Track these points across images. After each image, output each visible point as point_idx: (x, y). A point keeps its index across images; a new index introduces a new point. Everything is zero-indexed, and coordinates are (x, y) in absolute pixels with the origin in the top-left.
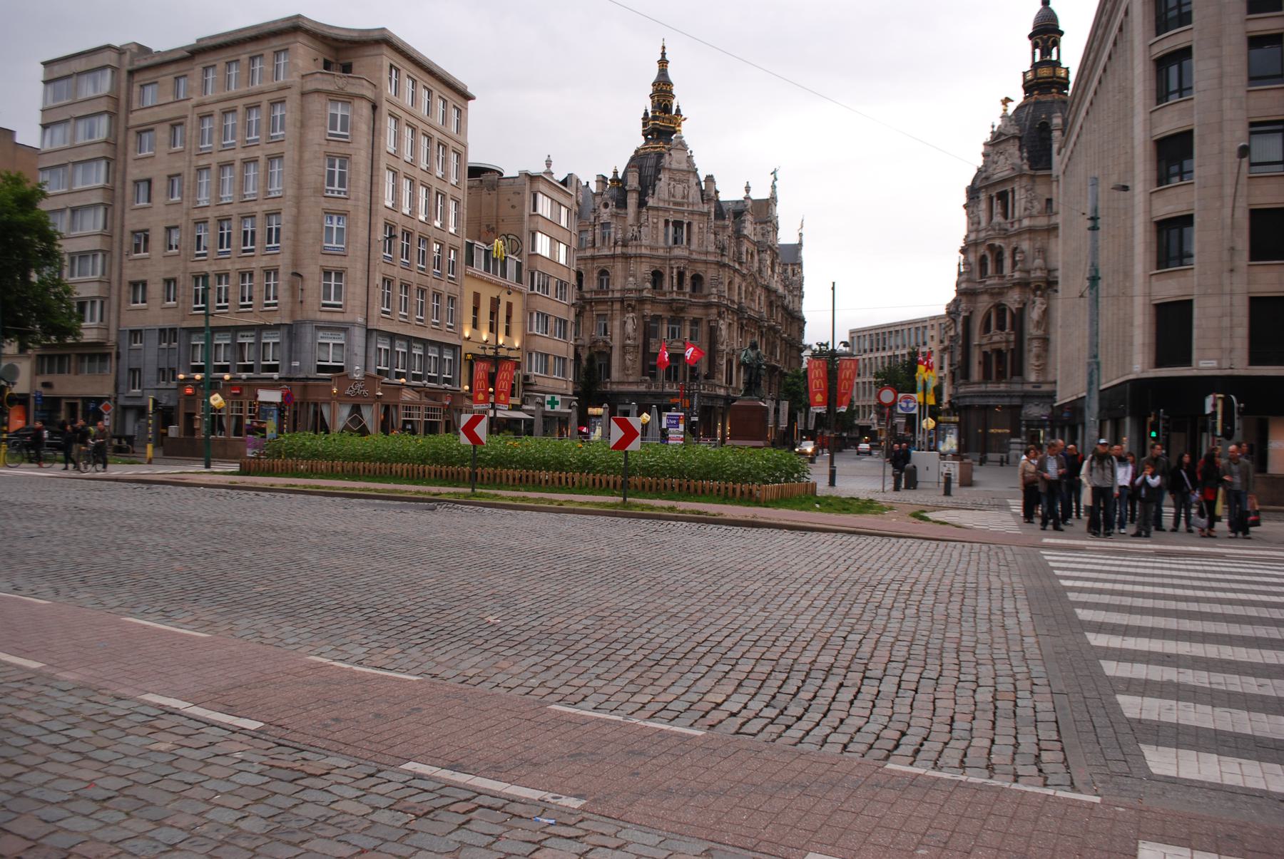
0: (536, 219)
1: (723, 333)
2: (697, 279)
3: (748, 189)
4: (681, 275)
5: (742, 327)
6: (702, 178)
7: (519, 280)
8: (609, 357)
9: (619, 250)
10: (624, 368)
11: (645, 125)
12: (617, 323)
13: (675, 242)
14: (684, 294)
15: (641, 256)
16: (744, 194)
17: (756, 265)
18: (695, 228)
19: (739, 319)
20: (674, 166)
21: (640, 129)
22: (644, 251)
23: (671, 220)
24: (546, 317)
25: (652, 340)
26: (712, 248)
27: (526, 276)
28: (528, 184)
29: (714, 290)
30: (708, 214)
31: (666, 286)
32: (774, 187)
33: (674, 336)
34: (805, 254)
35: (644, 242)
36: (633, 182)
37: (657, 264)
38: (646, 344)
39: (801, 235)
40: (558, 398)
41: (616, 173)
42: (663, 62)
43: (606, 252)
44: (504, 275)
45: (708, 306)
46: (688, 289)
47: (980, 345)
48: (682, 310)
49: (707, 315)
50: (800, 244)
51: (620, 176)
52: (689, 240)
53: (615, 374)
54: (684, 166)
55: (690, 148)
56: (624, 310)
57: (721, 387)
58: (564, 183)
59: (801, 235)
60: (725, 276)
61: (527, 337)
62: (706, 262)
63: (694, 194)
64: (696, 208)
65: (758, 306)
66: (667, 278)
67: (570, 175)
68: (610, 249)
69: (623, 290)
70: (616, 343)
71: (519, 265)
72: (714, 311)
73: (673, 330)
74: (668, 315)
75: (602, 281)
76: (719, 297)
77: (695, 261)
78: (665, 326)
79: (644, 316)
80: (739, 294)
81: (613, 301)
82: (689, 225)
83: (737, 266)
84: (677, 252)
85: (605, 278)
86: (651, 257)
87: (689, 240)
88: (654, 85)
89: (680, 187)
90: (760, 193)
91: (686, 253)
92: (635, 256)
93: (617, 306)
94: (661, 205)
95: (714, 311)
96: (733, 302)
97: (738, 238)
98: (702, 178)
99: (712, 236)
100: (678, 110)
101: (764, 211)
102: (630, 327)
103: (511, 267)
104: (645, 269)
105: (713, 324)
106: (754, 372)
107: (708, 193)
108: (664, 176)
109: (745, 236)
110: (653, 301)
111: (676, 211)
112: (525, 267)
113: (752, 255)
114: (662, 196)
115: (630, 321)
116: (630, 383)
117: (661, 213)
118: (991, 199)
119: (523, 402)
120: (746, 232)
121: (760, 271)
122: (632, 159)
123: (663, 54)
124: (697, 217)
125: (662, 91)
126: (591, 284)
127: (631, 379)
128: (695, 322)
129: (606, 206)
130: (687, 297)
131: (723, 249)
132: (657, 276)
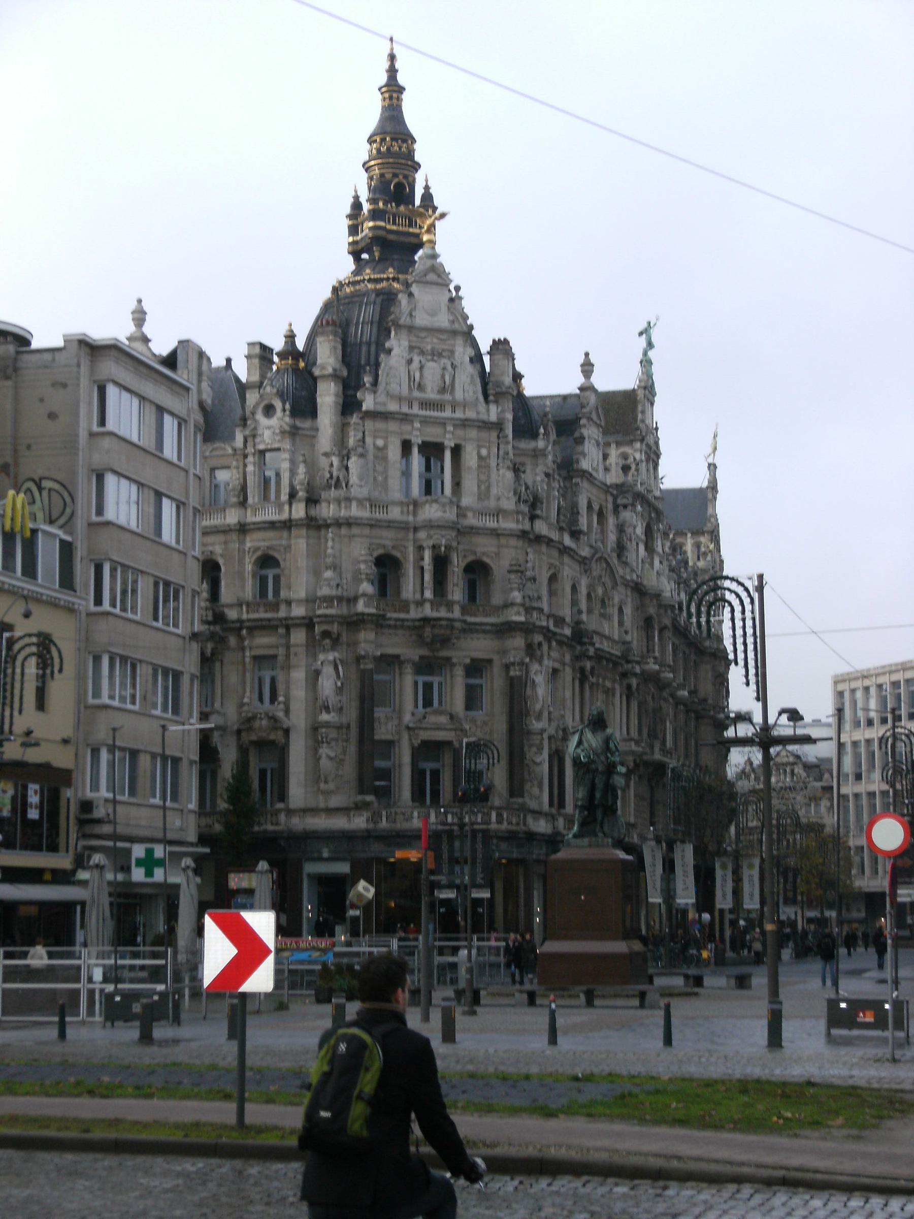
1: (541, 692)
2: (477, 571)
3: (587, 368)
4: (441, 563)
5: (583, 677)
6: (485, 347)
7: (67, 581)
8: (281, 752)
9: (299, 511)
10: (316, 776)
11: (353, 230)
12: (299, 675)
13: (428, 488)
14: (450, 606)
15: (349, 523)
16: (580, 380)
17: (612, 537)
18: (470, 459)
19: (577, 658)
20: (421, 319)
21: (344, 239)
22: (355, 511)
23: (417, 440)
24: (130, 664)
25: (380, 713)
26: (509, 504)
27: (83, 573)
28: (84, 370)
29: (517, 596)
30: (498, 426)
31: (409, 589)
32: (646, 363)
33: (428, 703)
34: (724, 509)
35: (355, 492)
36: (327, 357)
37: (387, 538)
38: (366, 722)
39: (712, 467)
40: (159, 851)
41: (291, 337)
42: (393, 90)
43: (270, 514)
44: (30, 571)
45: (505, 630)
46: (457, 593)
48: (445, 641)
49: (503, 652)
50: (713, 487)
51: (300, 344)
52: (457, 485)
53: (297, 793)
54: (443, 320)
55: (456, 278)
56: (313, 646)
57: (538, 813)
58: (171, 361)
59: (712, 467)
60: (539, 562)
62: (495, 533)
63: (466, 385)
64: (471, 414)
66: (410, 570)
67: (184, 344)
68: (280, 506)
69: (311, 600)
70: (298, 719)
71: (67, 549)
72: (518, 642)
73: (428, 687)
74: (411, 653)
75: (263, 581)
76: (528, 610)
77: (472, 531)
78: (409, 680)
79: (359, 659)
80: (574, 603)
81: (288, 625)
82: (457, 451)
83: (567, 541)
84: (431, 512)
85: (270, 573)
86: (373, 525)
87: (457, 485)
88: (371, 141)
89: (433, 369)
90: (617, 377)
92: (338, 523)
93: (299, 637)
94: (393, 407)
95: (518, 642)
96: (560, 622)
97: (568, 478)
98: (485, 346)
99: (510, 475)
100: (428, 197)
102: (327, 684)
103: (48, 556)
104: (357, 553)
107: (496, 375)
108: (398, 344)
109: (585, 474)
110: (379, 622)
111: (425, 421)
112: (80, 553)
113: (601, 514)
114: (394, 388)
115: (328, 670)
116: (330, 811)
117: (393, 426)
119: (80, 862)
120: (585, 464)
121: (621, 548)
122: (327, 307)
123: (392, 72)
124: (473, 433)
125: (394, 150)
126: (237, 588)
127: (335, 801)
128: (476, 668)
129: (269, 410)
130: (457, 613)
132: (387, 567)
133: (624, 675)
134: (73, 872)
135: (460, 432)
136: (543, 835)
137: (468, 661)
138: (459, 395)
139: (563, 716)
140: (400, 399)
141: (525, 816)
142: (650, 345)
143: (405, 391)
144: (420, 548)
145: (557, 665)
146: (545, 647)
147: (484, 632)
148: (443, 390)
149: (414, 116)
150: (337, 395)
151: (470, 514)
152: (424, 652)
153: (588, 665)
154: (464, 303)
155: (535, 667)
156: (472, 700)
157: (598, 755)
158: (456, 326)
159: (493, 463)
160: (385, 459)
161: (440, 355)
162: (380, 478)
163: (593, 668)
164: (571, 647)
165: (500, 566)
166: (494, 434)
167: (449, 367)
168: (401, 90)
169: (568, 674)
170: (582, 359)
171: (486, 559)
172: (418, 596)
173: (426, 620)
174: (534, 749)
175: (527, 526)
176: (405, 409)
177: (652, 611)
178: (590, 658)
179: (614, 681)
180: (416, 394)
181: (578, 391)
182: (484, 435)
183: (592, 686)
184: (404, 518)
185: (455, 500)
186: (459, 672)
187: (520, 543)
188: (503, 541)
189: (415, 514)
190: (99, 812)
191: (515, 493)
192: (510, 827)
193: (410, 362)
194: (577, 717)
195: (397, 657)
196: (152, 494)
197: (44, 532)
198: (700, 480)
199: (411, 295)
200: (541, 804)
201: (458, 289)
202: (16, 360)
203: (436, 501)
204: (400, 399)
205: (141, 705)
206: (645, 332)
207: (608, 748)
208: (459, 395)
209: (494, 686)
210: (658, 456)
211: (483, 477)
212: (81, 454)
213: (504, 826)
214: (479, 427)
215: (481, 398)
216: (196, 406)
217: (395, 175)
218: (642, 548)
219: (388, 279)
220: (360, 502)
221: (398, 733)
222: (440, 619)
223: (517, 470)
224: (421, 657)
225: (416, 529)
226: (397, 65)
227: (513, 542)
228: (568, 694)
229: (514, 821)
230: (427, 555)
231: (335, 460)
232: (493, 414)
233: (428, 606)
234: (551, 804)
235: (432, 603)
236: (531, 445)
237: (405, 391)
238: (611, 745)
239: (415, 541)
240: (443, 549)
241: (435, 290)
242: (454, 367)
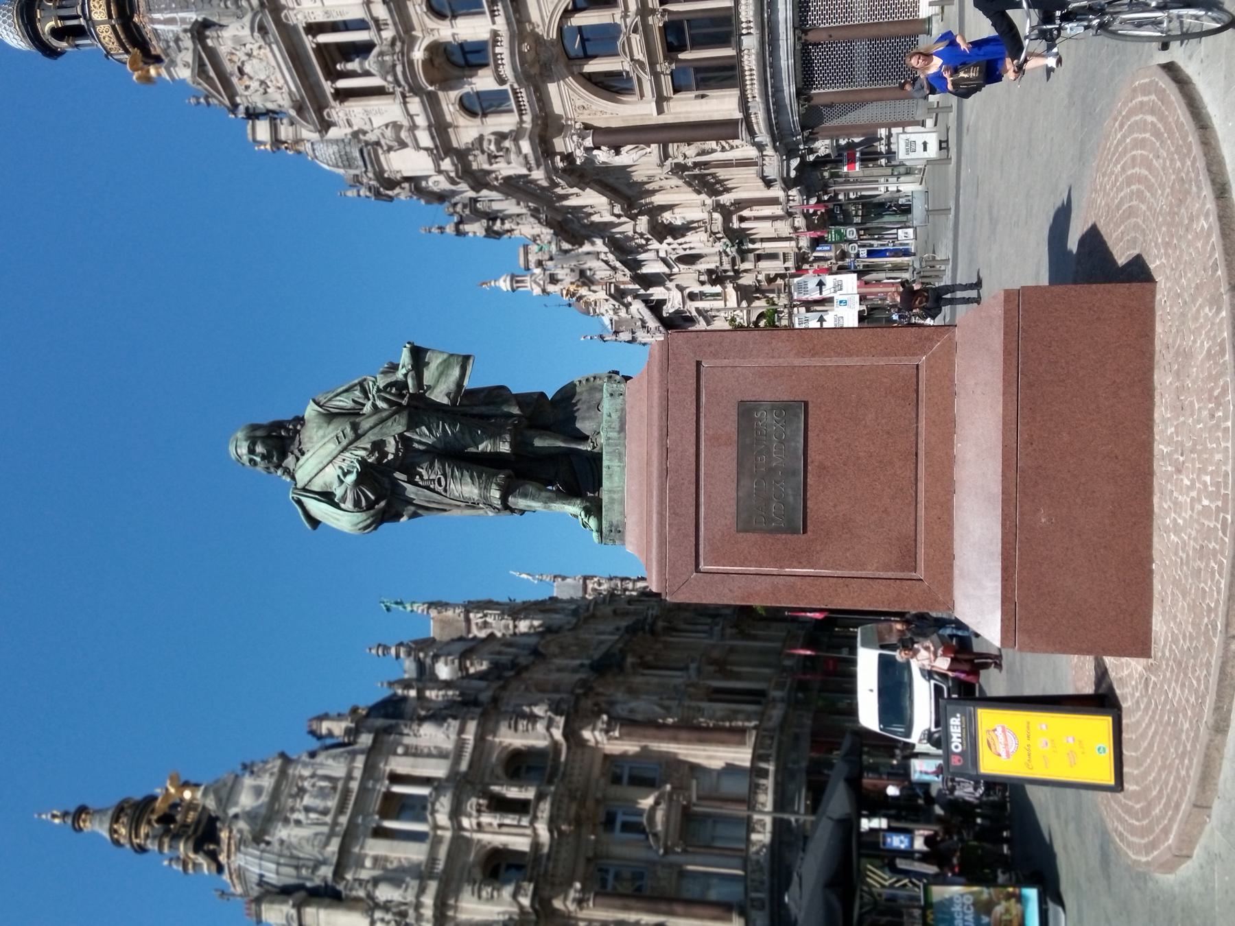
31: (521, 843)
47: (661, 100)
64: (360, 762)
82: (396, 778)
87: (426, 781)
118: (343, 95)
133: (653, 632)
143: (325, 829)
150: (319, 906)
157: (358, 437)
169: (638, 680)
180: (328, 819)
185: (436, 784)
195: (589, 860)
199: (236, 816)
203: (433, 804)
217: (149, 822)
219: (229, 838)
220: (422, 890)
221: (671, 865)
231: (378, 914)
239: (473, 831)
240: (481, 801)
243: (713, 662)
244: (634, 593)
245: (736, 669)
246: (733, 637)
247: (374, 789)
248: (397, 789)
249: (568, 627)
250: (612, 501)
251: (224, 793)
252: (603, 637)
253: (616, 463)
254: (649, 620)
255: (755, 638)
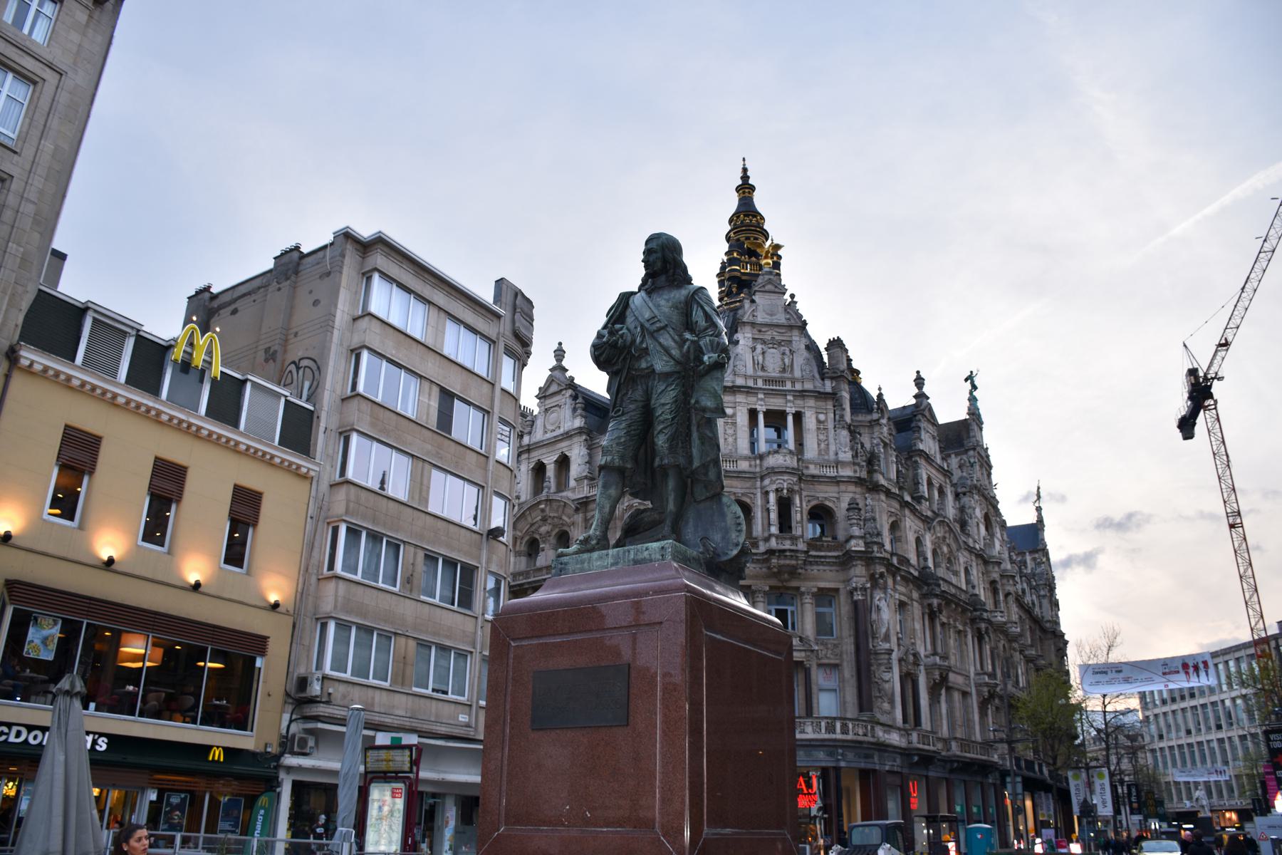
0: (364, 323)
2: (820, 514)
4: (785, 506)
5: (932, 615)
14: (794, 539)
18: (810, 421)
19: (924, 596)
20: (760, 320)
23: (761, 408)
26: (846, 456)
29: (856, 531)
31: (758, 529)
32: (972, 400)
39: (1039, 509)
42: (745, 189)
48: (793, 572)
50: (1040, 520)
54: (781, 318)
57: (889, 727)
59: (1039, 509)
61: (312, 576)
62: (836, 481)
64: (809, 386)
65: (965, 577)
82: (798, 417)
88: (731, 221)
90: (948, 410)
91: (791, 462)
94: (740, 382)
98: (822, 345)
101: (963, 438)
105: (858, 597)
106: (665, 399)
108: (744, 337)
109: (922, 454)
117: (740, 398)
123: (745, 177)
124: (811, 402)
128: (825, 597)
131: (872, 460)
134: (277, 757)
135: (799, 402)
136: (895, 747)
137: (815, 590)
138: (797, 374)
139: (913, 644)
140: (746, 377)
141: (873, 728)
142: (974, 387)
143: (750, 371)
144: (767, 493)
145: (903, 598)
146: (890, 581)
147: (828, 564)
148: (784, 370)
149: (761, 202)
151: (812, 467)
152: (774, 582)
153: (935, 602)
154: (798, 306)
155: (878, 595)
156: (823, 627)
158: (792, 322)
159: (830, 425)
160: (734, 424)
161: (780, 344)
162: (730, 440)
163: (939, 605)
164: (919, 588)
165: (841, 509)
166: (830, 405)
167: (787, 352)
168: (752, 188)
169: (916, 609)
170: (915, 376)
171: (830, 504)
172: (766, 534)
173: (771, 552)
174: (883, 668)
175: (864, 475)
176: (750, 383)
177: (996, 576)
178: (937, 596)
179: (965, 624)
180: (760, 373)
181: (914, 401)
182: (820, 404)
183: (943, 625)
184: (752, 470)
186: (808, 599)
187: (858, 490)
188: (843, 487)
189: (761, 466)
190: (316, 688)
191: (852, 448)
192: (855, 738)
193: (754, 349)
194: (929, 647)
196: (436, 390)
197: (254, 384)
198: (1031, 519)
199: (753, 301)
200: (894, 719)
201: (792, 296)
202: (298, 264)
204: (746, 377)
205: (402, 585)
206: (970, 378)
207: (689, 325)
208: (797, 374)
209: (841, 614)
210: (990, 467)
211: (822, 437)
212: (336, 333)
213: (850, 737)
214: (816, 397)
215: (817, 376)
216: (508, 333)
218: (982, 528)
222: (784, 551)
223: (853, 432)
224: (771, 587)
225: (762, 478)
226: (749, 173)
227: (852, 488)
228: (918, 626)
229: (861, 732)
230: (772, 497)
232: (828, 386)
233: (773, 541)
234: (905, 720)
235: (777, 537)
236: (869, 418)
237: (750, 371)
238: (697, 316)
239: (762, 488)
241: (773, 296)
242: (792, 352)
243: (944, 679)
244: (963, 597)
245: (943, 698)
246: (979, 693)
247: (787, 401)
248: (790, 419)
249: (971, 542)
250: (582, 562)
251: (769, 287)
252: (963, 575)
253: (610, 560)
254: (985, 615)
255: (983, 714)
